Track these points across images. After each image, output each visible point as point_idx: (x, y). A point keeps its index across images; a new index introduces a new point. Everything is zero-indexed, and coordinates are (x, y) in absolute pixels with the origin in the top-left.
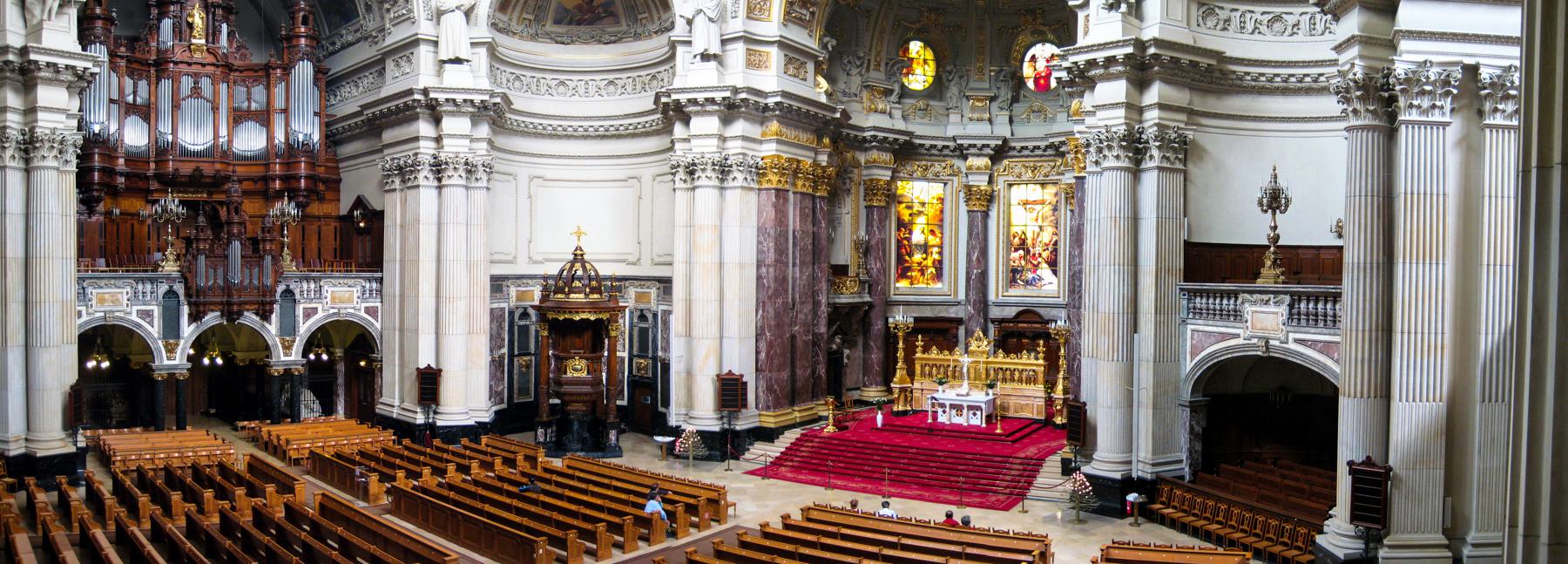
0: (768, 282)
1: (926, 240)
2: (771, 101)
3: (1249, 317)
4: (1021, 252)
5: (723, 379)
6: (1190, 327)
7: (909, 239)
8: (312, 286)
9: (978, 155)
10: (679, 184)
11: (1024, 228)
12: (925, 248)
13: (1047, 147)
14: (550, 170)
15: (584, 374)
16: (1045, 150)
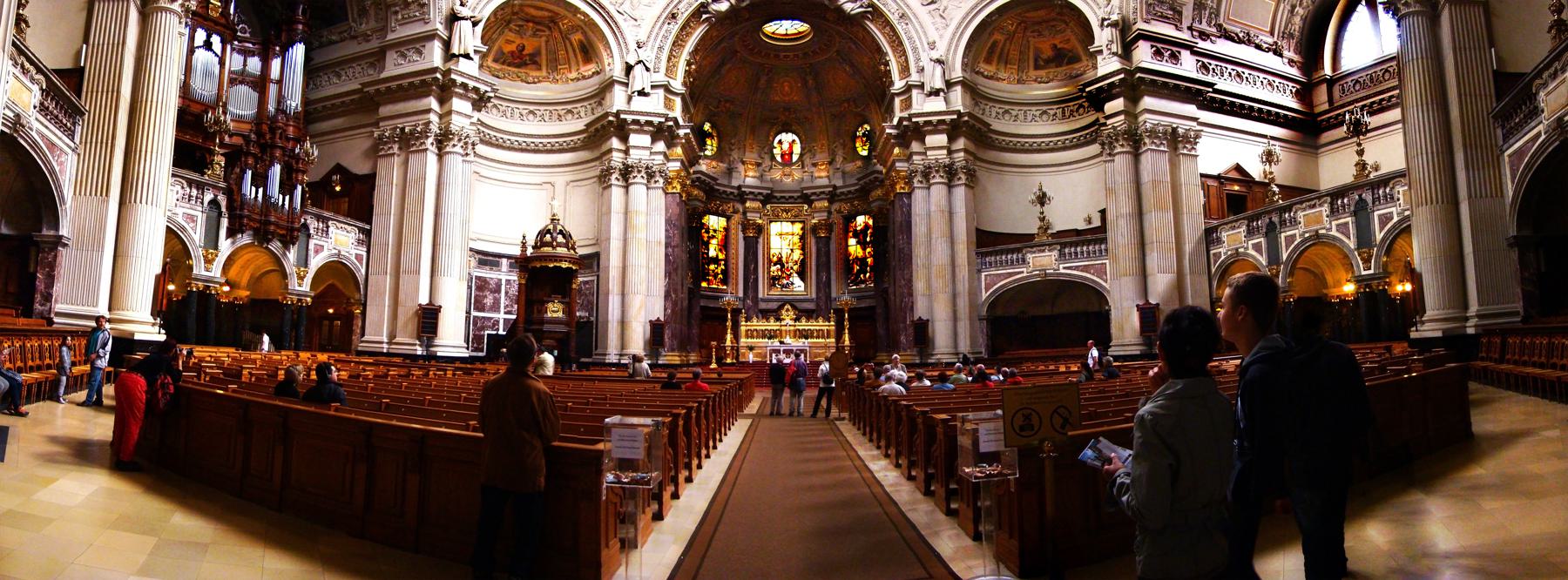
0: (673, 258)
1: (717, 256)
2: (681, 132)
3: (1031, 261)
4: (779, 266)
5: (654, 324)
6: (983, 274)
7: (708, 254)
8: (321, 225)
9: (753, 200)
10: (614, 181)
11: (780, 251)
12: (716, 260)
13: (798, 197)
14: (485, 169)
15: (560, 314)
16: (796, 199)
